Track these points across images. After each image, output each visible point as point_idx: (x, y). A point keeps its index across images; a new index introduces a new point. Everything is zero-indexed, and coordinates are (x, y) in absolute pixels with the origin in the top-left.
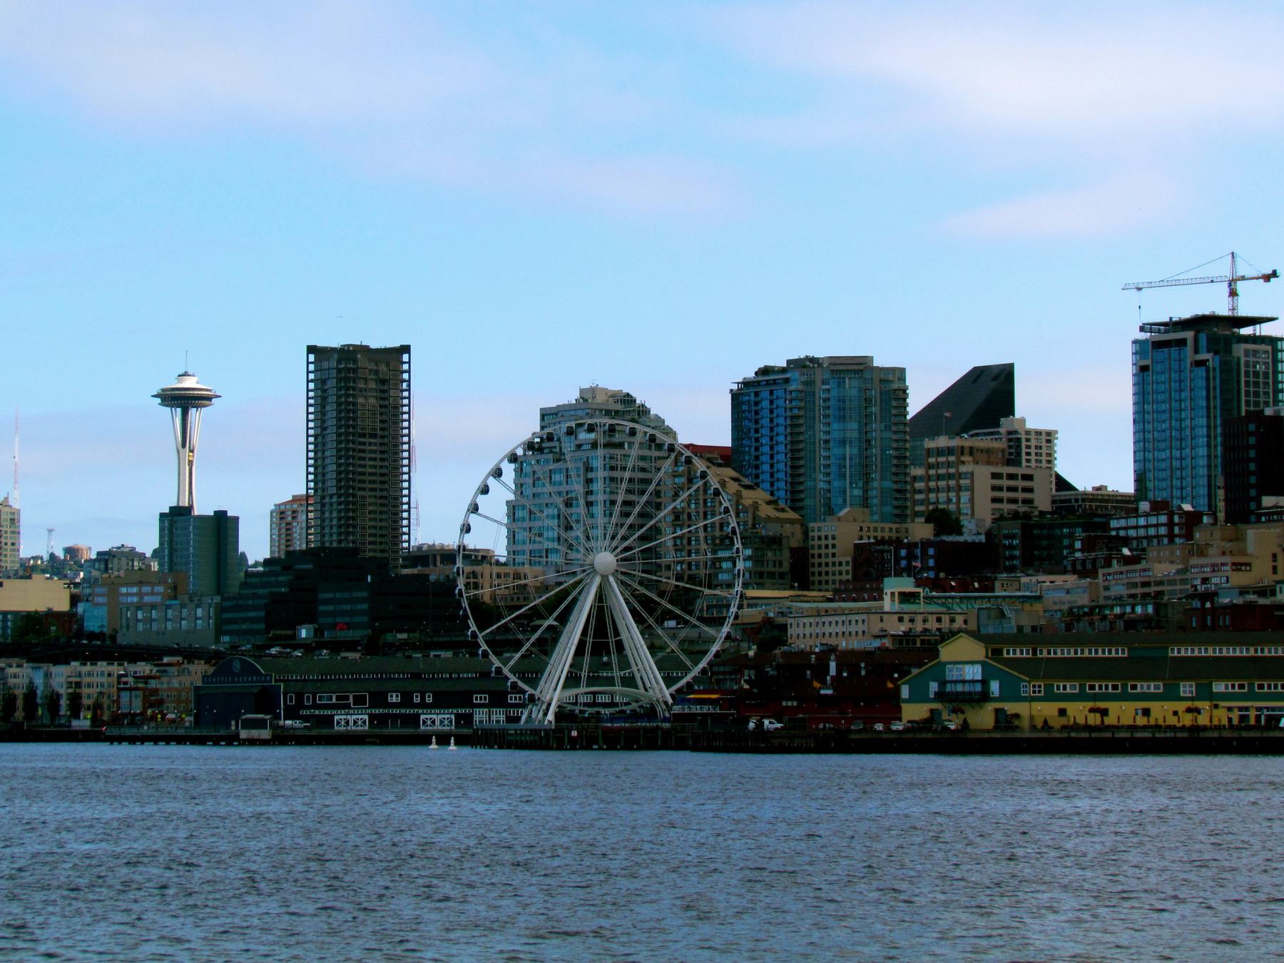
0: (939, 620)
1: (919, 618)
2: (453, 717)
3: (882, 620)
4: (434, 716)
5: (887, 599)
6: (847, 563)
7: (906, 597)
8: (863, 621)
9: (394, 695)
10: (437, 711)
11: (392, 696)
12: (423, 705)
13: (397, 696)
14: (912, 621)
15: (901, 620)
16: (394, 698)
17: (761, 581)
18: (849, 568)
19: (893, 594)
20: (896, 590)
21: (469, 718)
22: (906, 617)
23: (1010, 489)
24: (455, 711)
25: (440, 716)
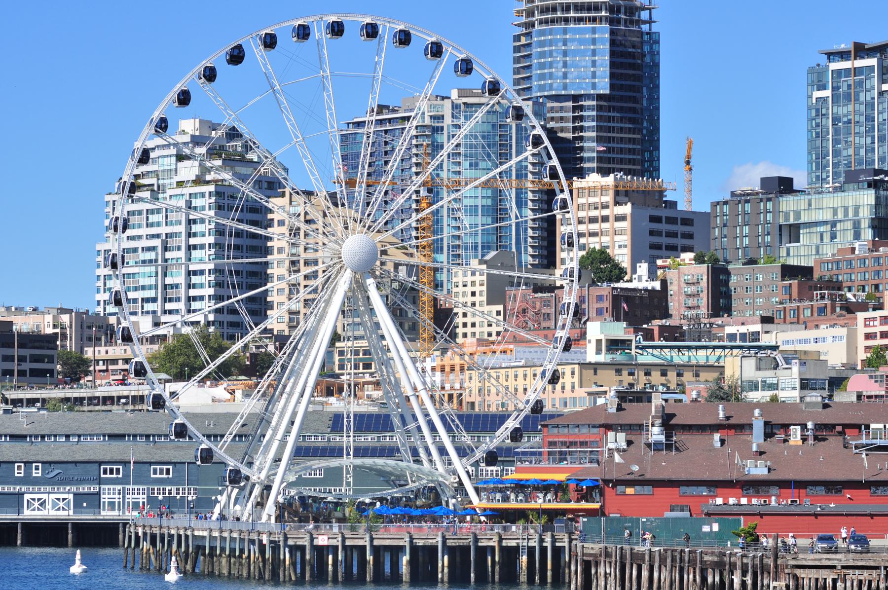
2: (71, 496)
4: (44, 496)
5: (591, 348)
6: (498, 313)
7: (615, 345)
8: (573, 373)
10: (49, 488)
12: (28, 480)
19: (599, 342)
21: (94, 500)
23: (670, 235)
24: (74, 489)
25: (53, 496)
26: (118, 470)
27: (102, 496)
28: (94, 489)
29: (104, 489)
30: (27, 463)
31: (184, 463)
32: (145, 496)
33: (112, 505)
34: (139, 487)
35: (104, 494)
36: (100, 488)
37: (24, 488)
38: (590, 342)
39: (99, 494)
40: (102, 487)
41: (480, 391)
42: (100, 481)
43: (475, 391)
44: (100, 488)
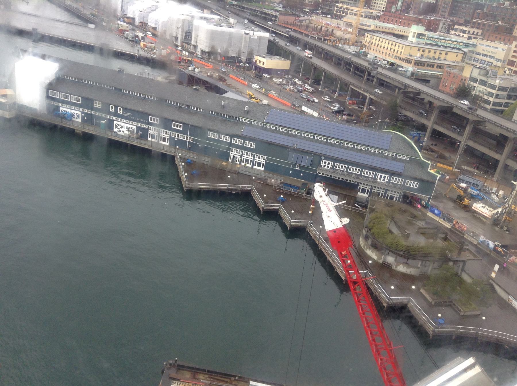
0: (435, 53)
1: (427, 51)
3: (411, 49)
4: (123, 124)
7: (420, 36)
9: (98, 102)
10: (125, 121)
11: (96, 103)
12: (116, 114)
13: (99, 104)
14: (423, 51)
15: (419, 50)
16: (97, 105)
17: (355, 3)
18: (386, 3)
19: (415, 33)
20: (417, 32)
22: (421, 50)
24: (136, 124)
26: (157, 120)
27: (149, 131)
28: (146, 126)
29: (150, 128)
30: (116, 107)
31: (188, 125)
32: (169, 136)
33: (153, 137)
34: (166, 131)
35: (150, 130)
36: (148, 127)
37: (114, 118)
38: (411, 32)
39: (147, 129)
40: (150, 126)
41: (369, 42)
42: (149, 124)
43: (368, 42)
44: (148, 127)
